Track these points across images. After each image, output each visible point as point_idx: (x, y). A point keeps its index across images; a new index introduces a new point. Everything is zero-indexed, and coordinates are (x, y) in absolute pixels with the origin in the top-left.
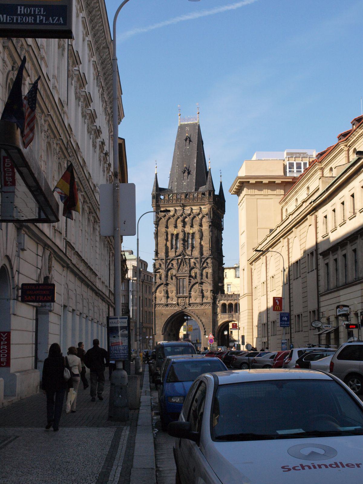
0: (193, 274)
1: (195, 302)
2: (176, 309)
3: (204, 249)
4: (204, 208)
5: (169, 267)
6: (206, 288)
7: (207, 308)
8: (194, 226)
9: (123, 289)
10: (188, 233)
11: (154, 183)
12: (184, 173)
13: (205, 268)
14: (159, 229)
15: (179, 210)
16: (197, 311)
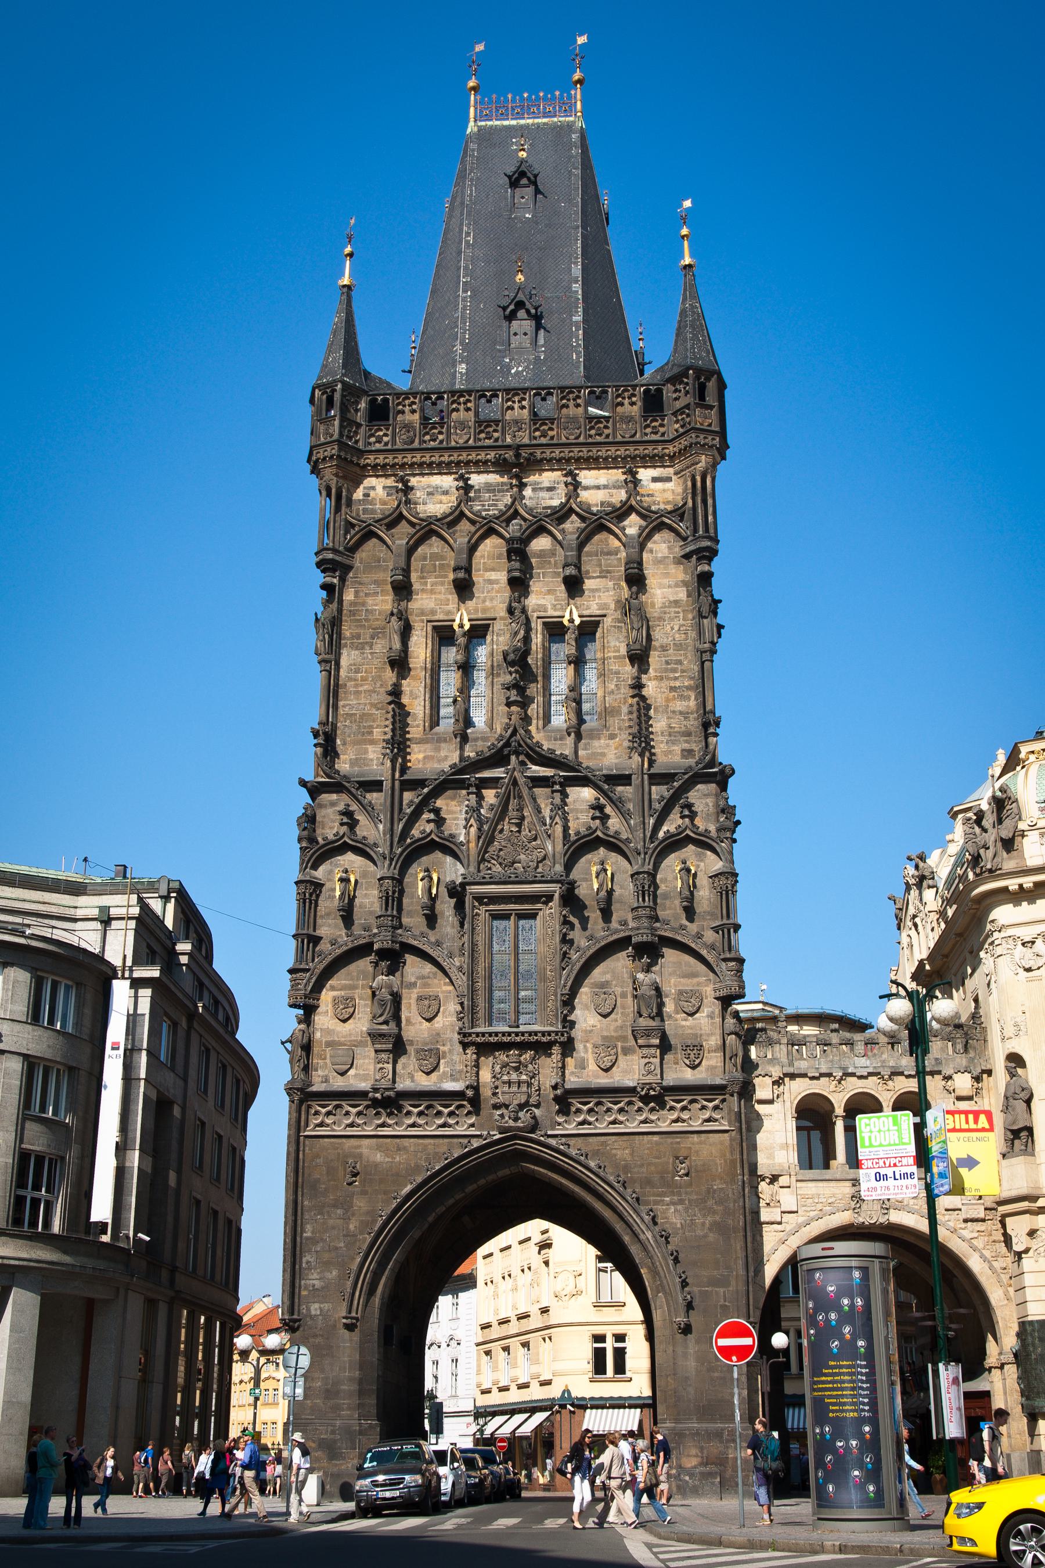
0: (589, 887)
1: (603, 1080)
2: (460, 1130)
3: (659, 724)
4: (655, 480)
5: (415, 832)
6: (687, 984)
7: (696, 1125)
8: (589, 584)
9: (70, 1029)
10: (555, 630)
11: (335, 333)
12: (511, 317)
13: (675, 843)
14: (349, 596)
15: (489, 488)
16: (621, 1151)
